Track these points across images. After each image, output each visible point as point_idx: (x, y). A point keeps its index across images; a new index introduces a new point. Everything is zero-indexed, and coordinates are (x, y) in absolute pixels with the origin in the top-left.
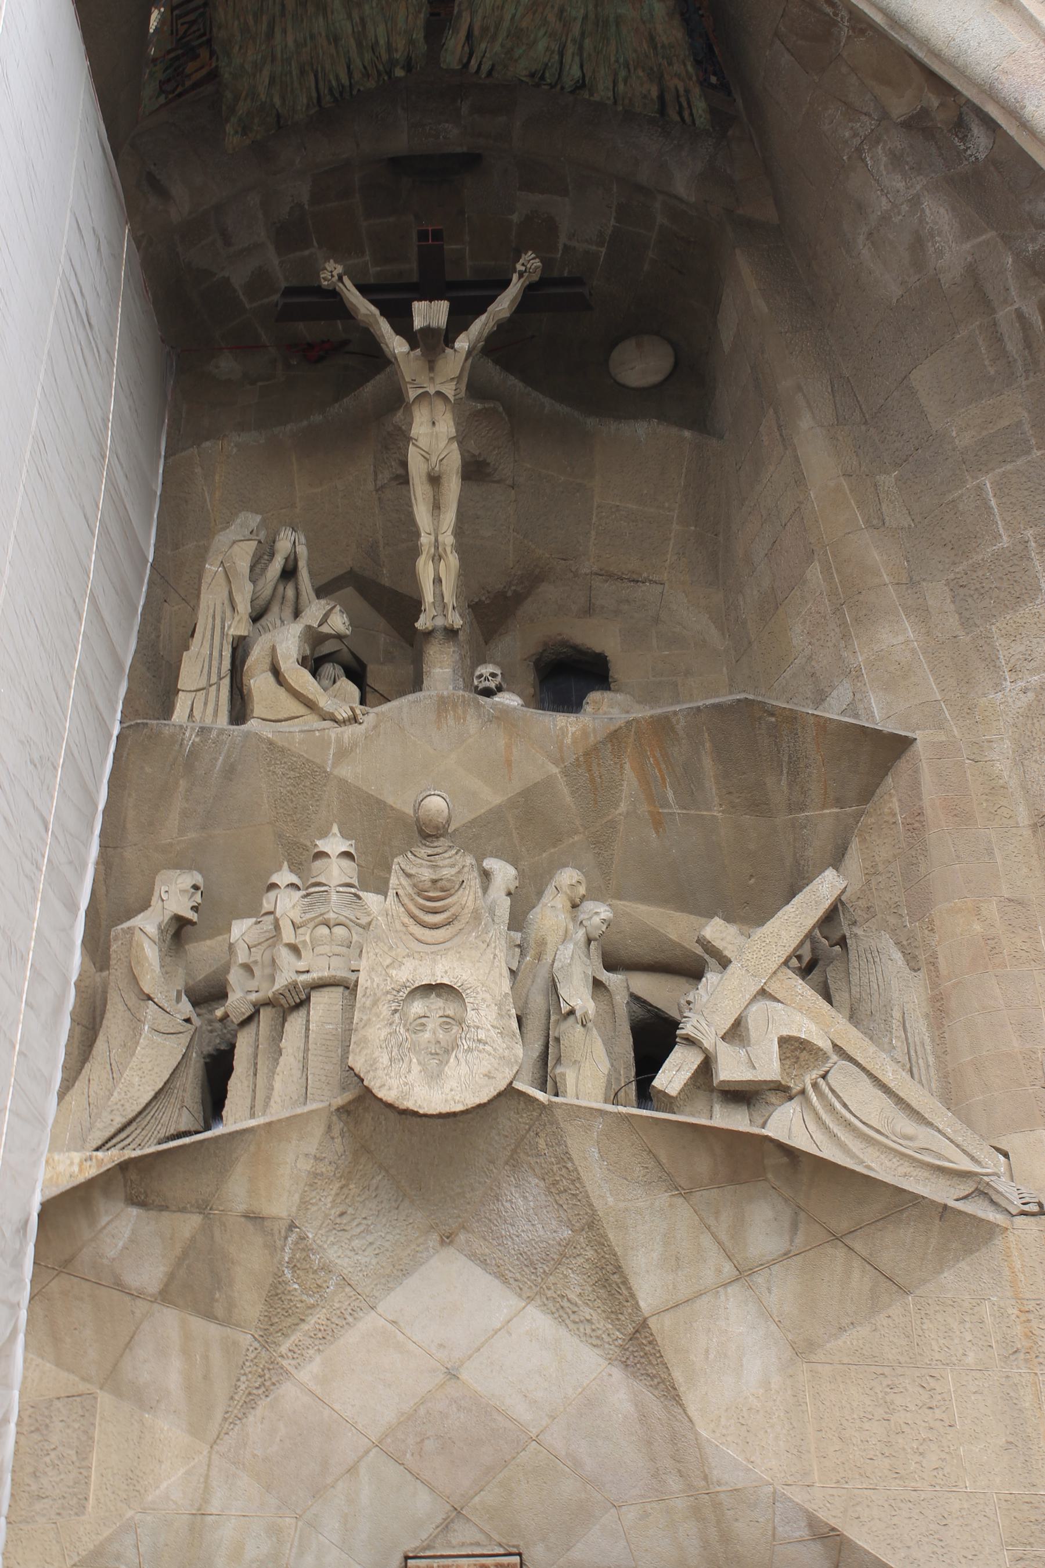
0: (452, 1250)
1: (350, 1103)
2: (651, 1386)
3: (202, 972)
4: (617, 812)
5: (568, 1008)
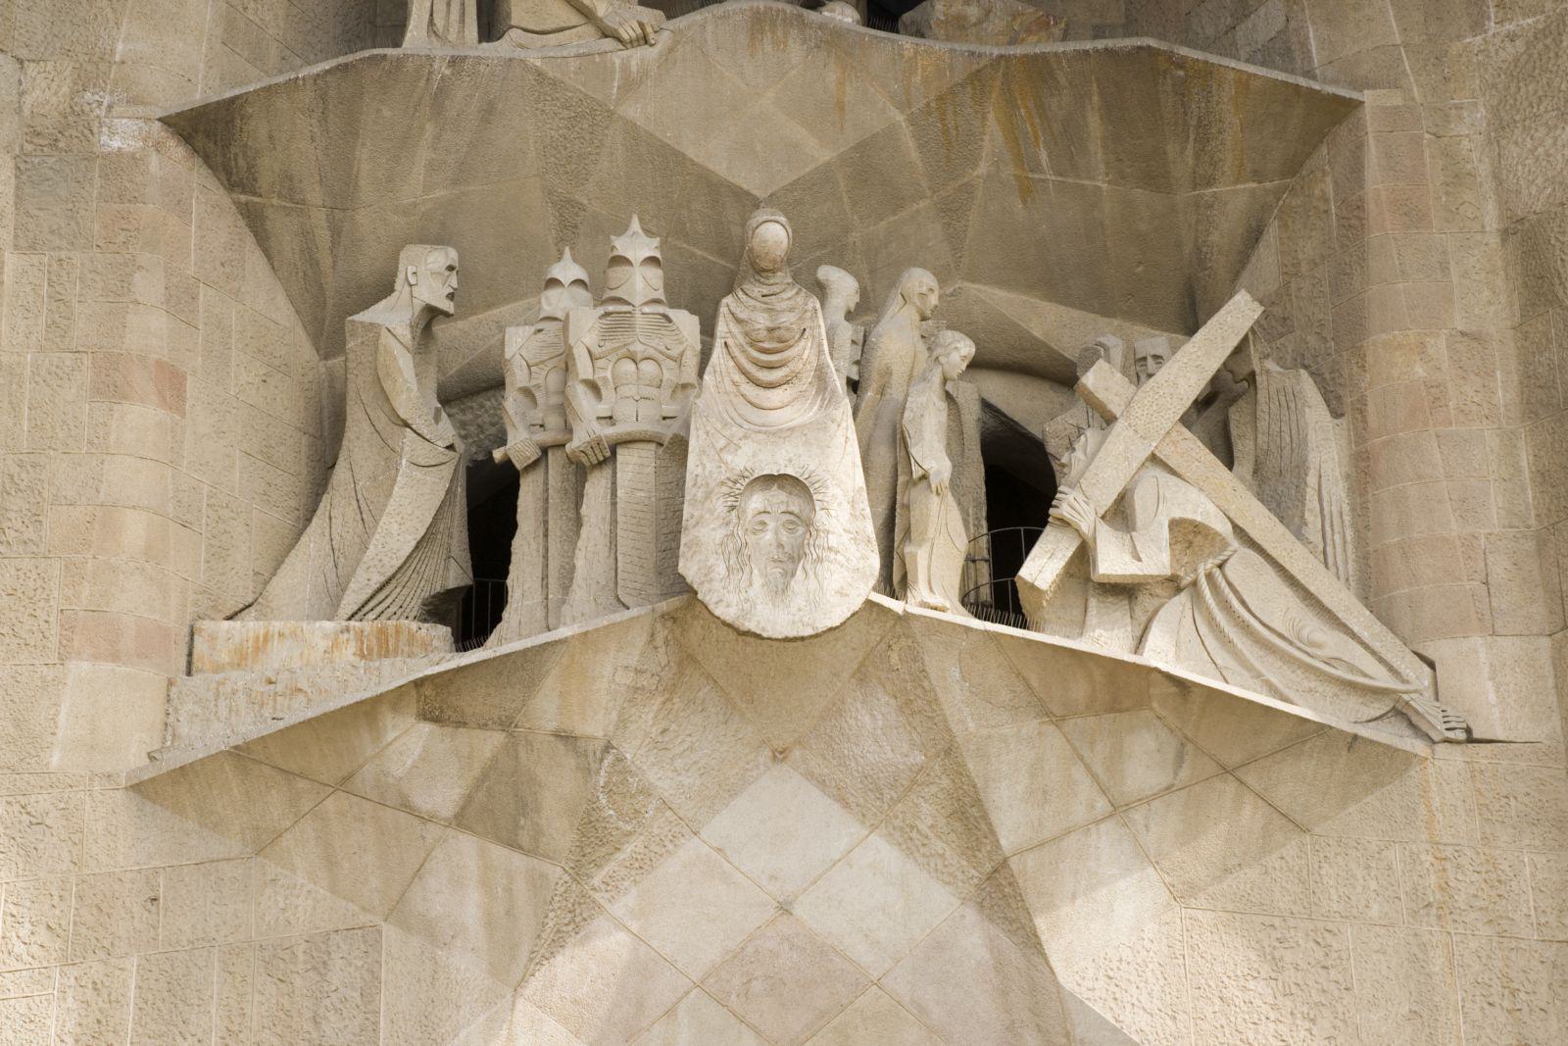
0: (785, 767)
2: (1009, 931)
4: (976, 173)
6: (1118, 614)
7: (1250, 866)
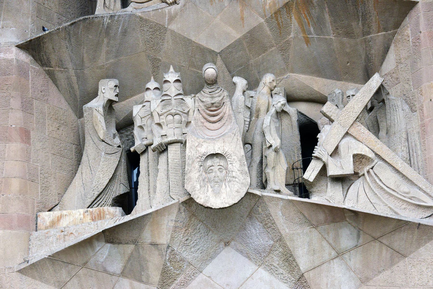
0: (229, 247)
1: (186, 200)
3: (122, 116)
4: (290, 37)
5: (269, 145)
6: (338, 187)
7: (387, 270)
